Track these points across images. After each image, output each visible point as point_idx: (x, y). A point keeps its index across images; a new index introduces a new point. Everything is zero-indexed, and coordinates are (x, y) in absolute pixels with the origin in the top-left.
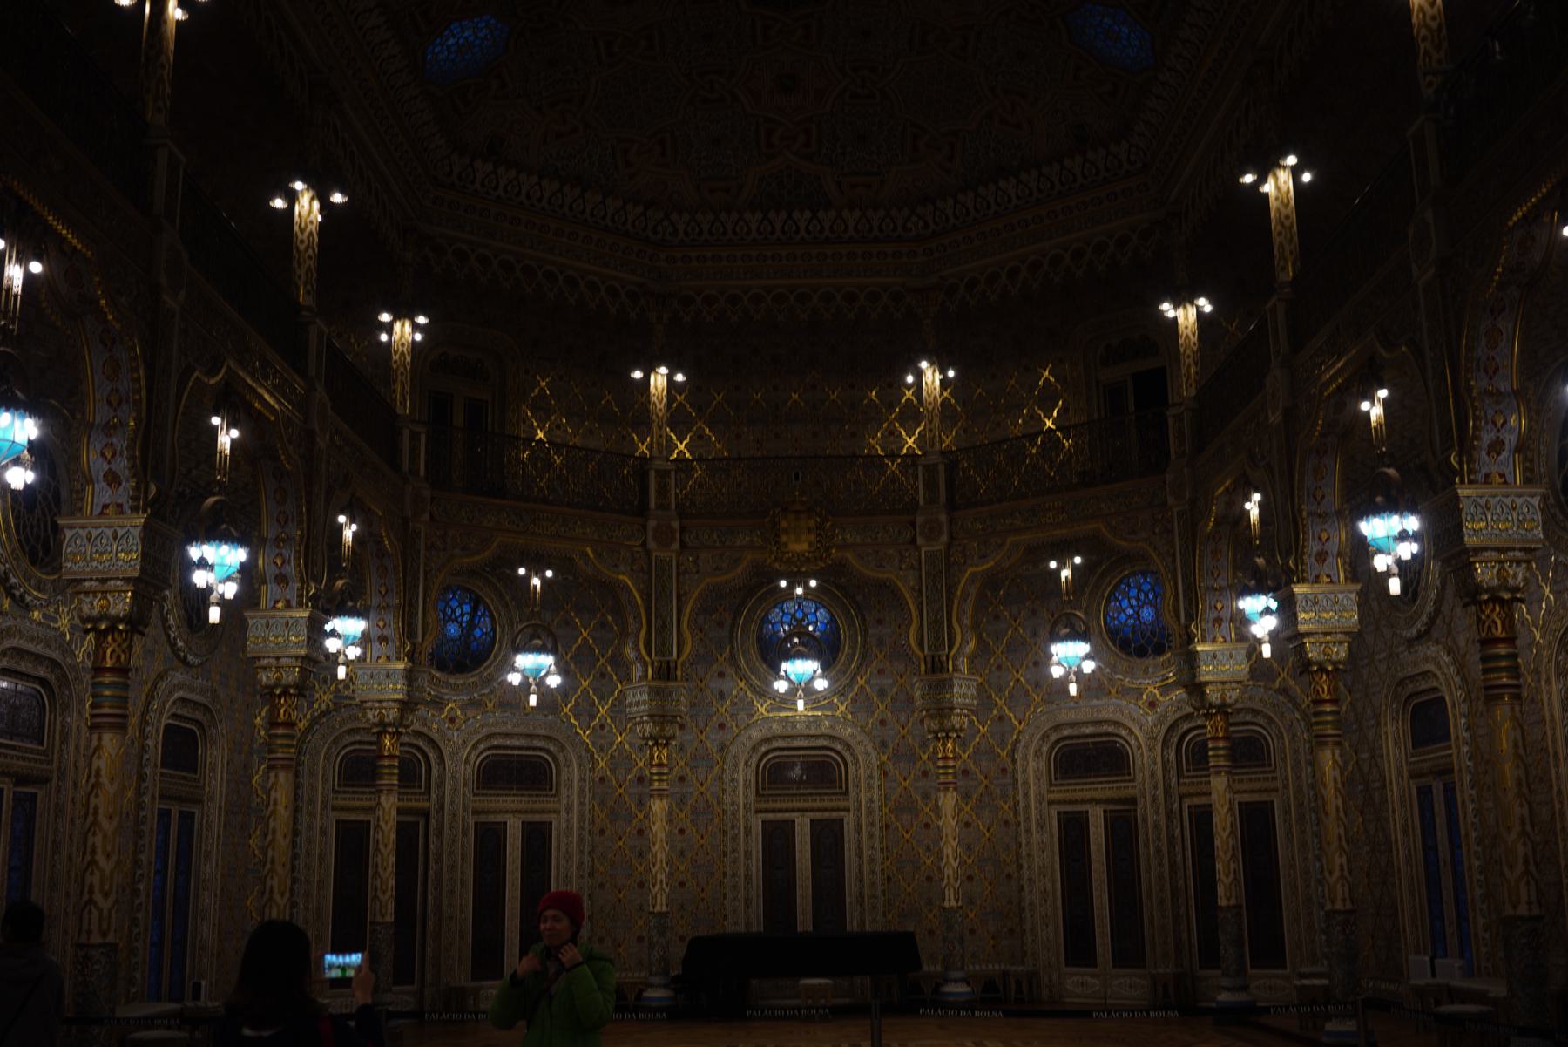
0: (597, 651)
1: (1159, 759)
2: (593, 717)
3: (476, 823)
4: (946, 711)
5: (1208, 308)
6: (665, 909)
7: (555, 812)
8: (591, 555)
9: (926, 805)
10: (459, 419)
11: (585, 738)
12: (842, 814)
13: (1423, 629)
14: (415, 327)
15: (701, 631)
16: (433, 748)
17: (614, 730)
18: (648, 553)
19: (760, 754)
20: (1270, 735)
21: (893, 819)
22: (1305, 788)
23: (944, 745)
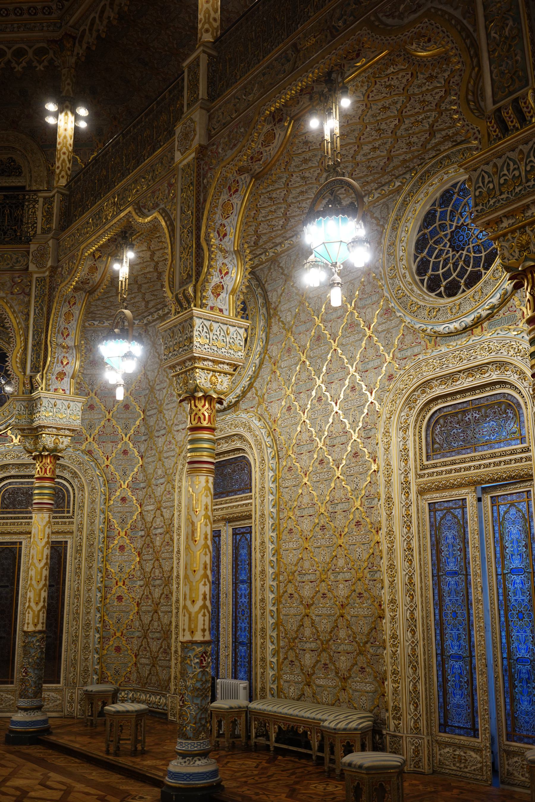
5: (83, 125)
13: (233, 401)
20: (72, 487)
22: (97, 532)
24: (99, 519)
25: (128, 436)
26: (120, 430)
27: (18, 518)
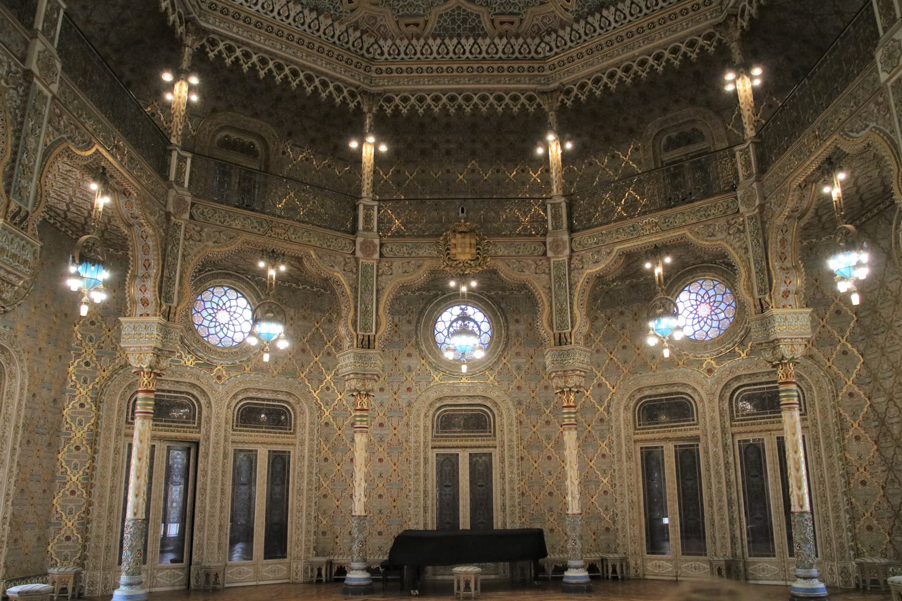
0: (325, 338)
1: (717, 409)
2: (322, 382)
3: (235, 450)
4: (571, 372)
6: (363, 514)
7: (292, 444)
8: (314, 257)
9: (549, 444)
11: (315, 395)
12: (491, 449)
14: (191, 88)
15: (396, 326)
16: (204, 396)
17: (336, 391)
18: (357, 259)
19: (435, 409)
21: (526, 453)
22: (831, 426)
23: (568, 397)
24: (831, 414)
25: (845, 337)
26: (836, 334)
27: (757, 419)
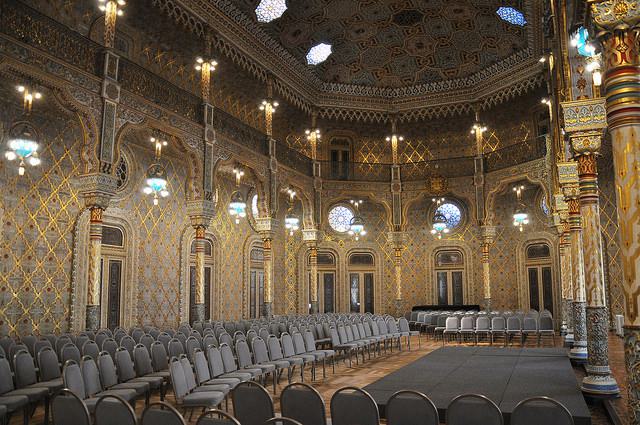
10: (340, 157)
